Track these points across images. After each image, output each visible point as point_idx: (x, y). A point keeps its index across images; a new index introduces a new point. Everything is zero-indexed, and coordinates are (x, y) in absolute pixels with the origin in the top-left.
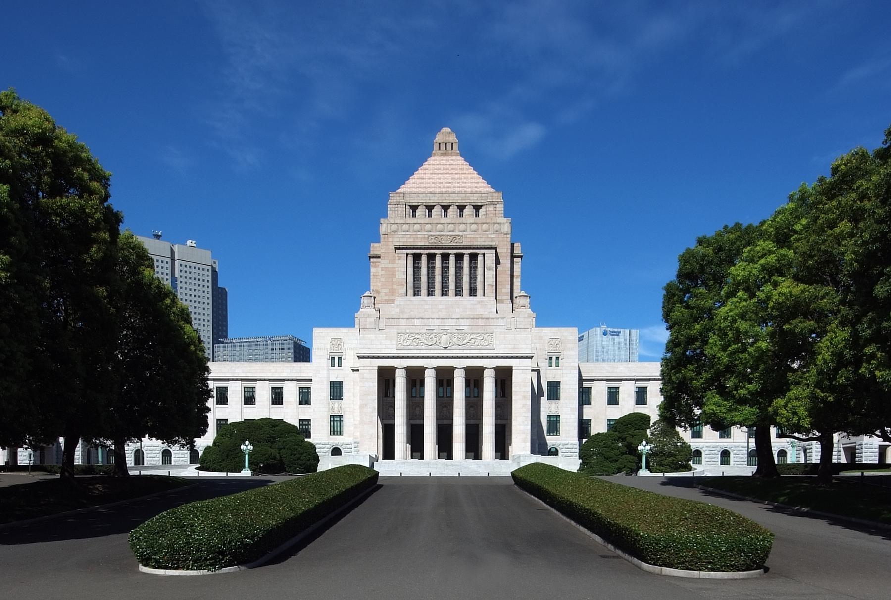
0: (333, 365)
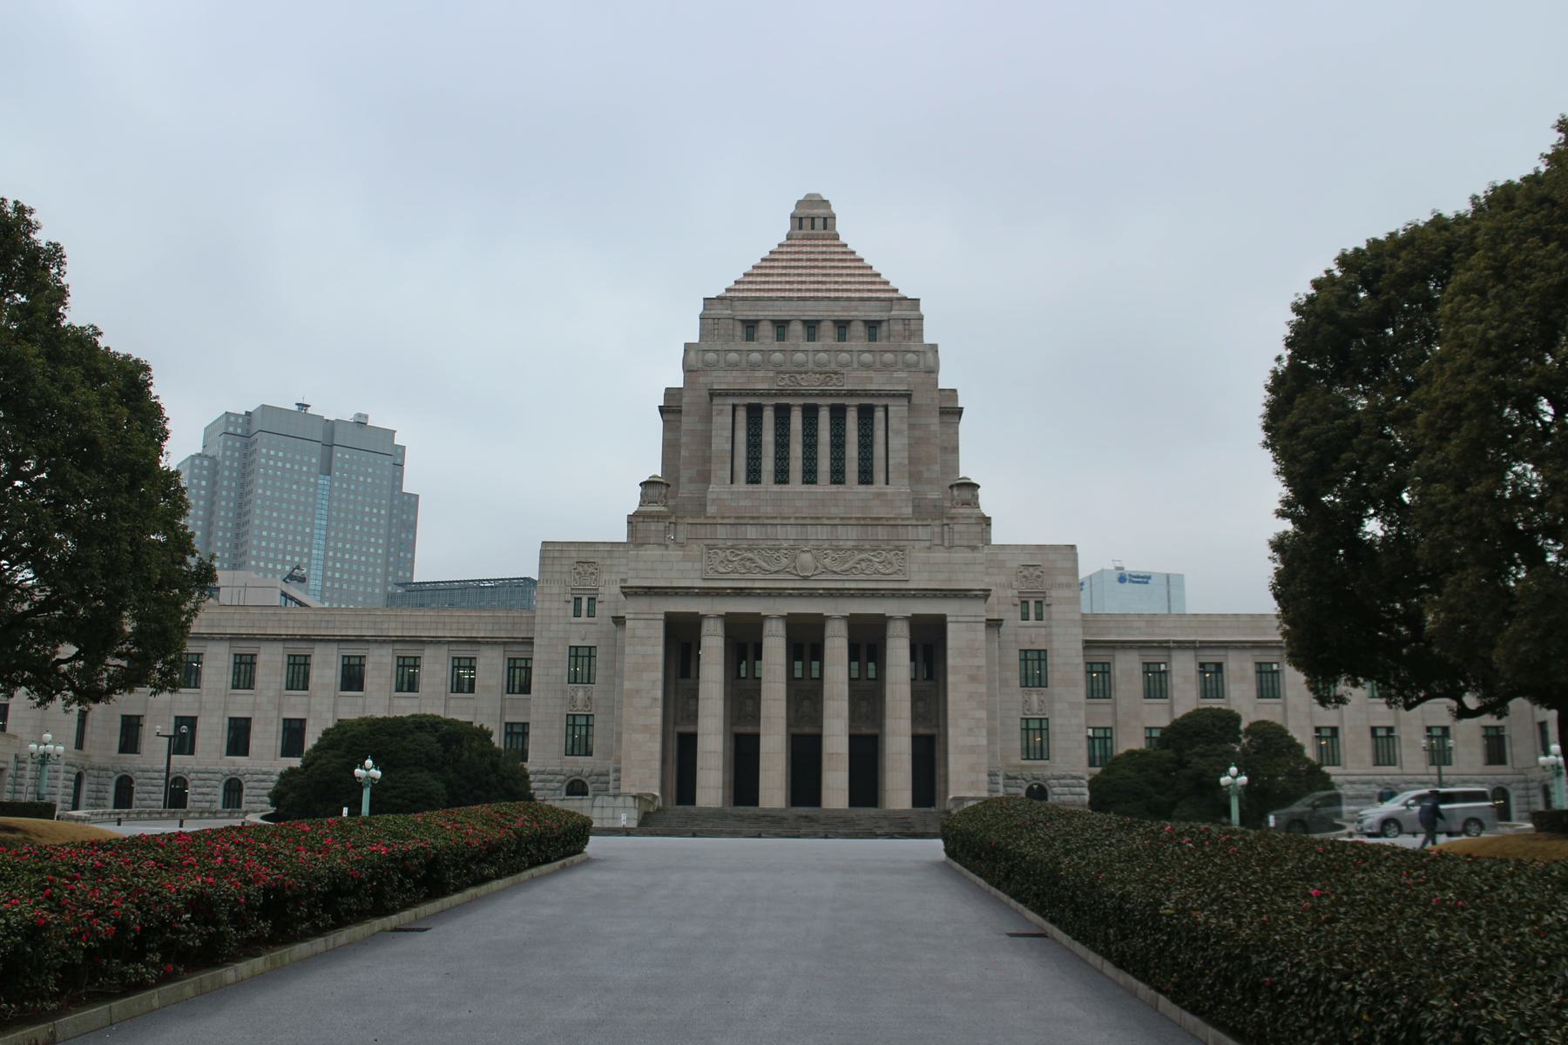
0: (577, 614)
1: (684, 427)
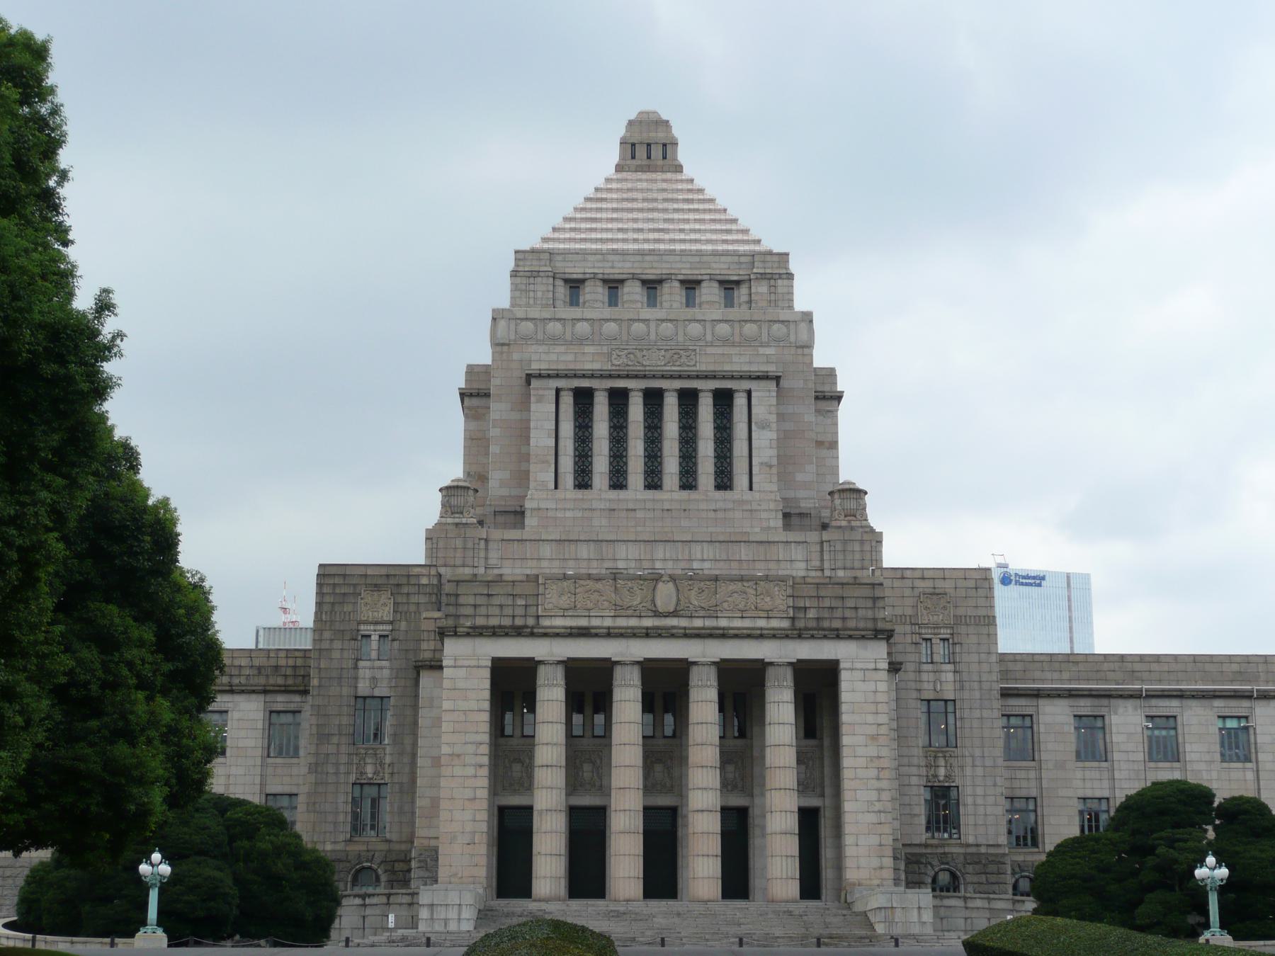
1: (494, 415)
